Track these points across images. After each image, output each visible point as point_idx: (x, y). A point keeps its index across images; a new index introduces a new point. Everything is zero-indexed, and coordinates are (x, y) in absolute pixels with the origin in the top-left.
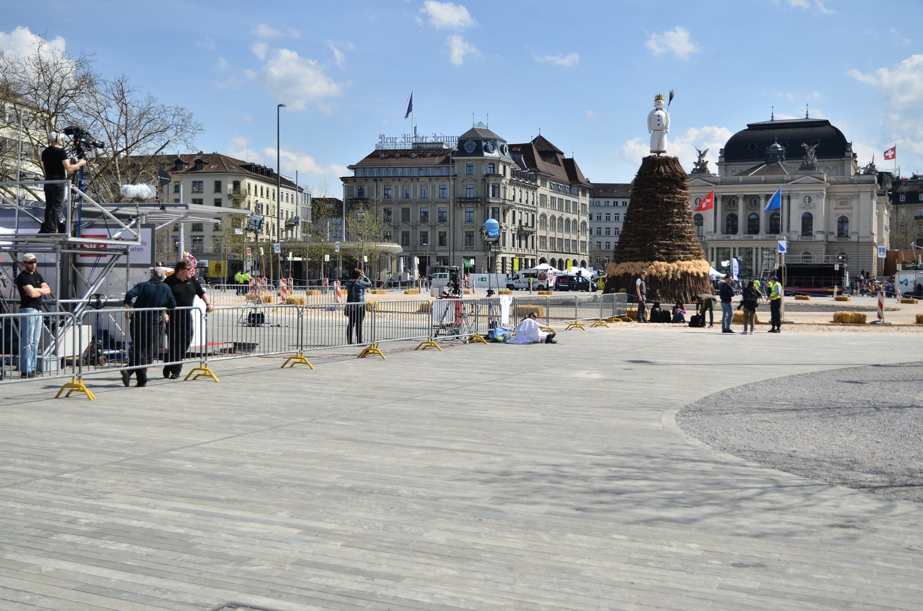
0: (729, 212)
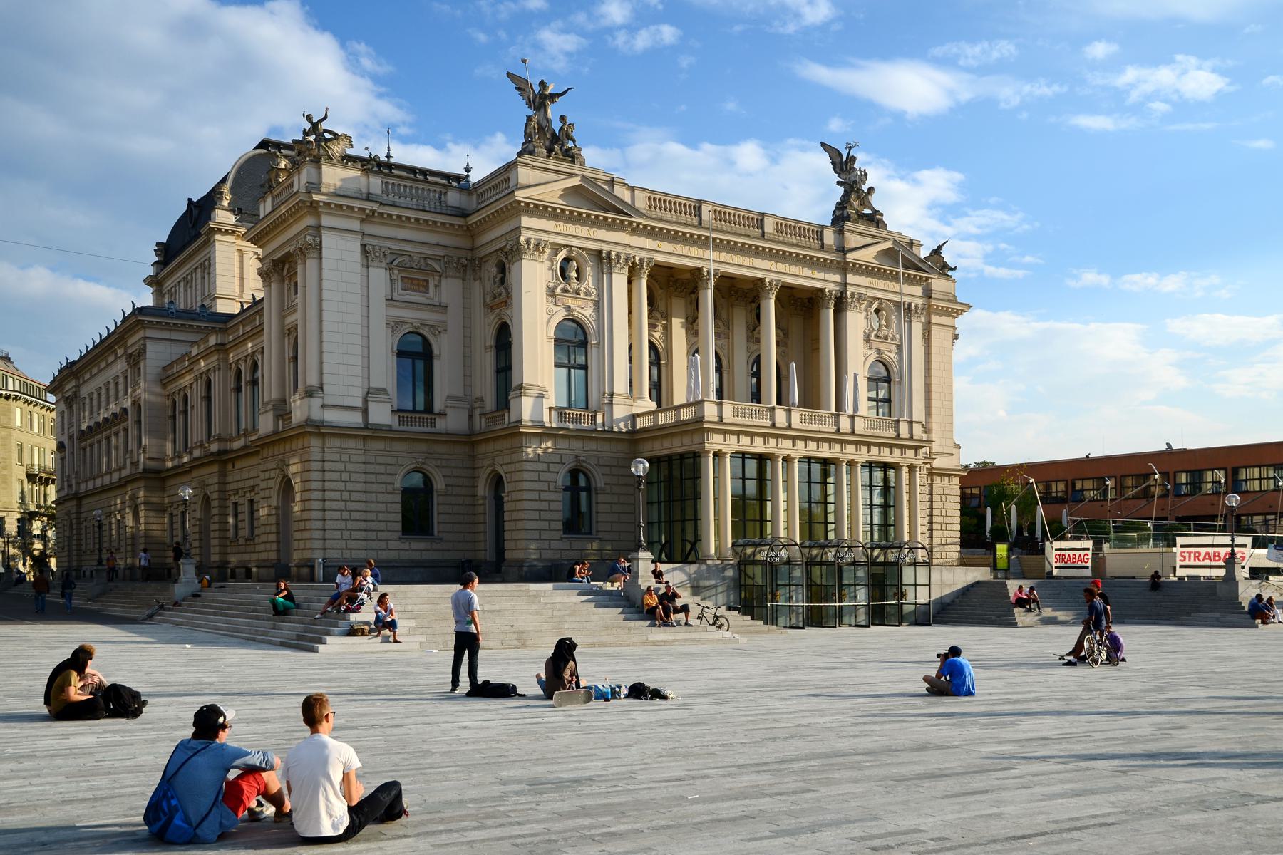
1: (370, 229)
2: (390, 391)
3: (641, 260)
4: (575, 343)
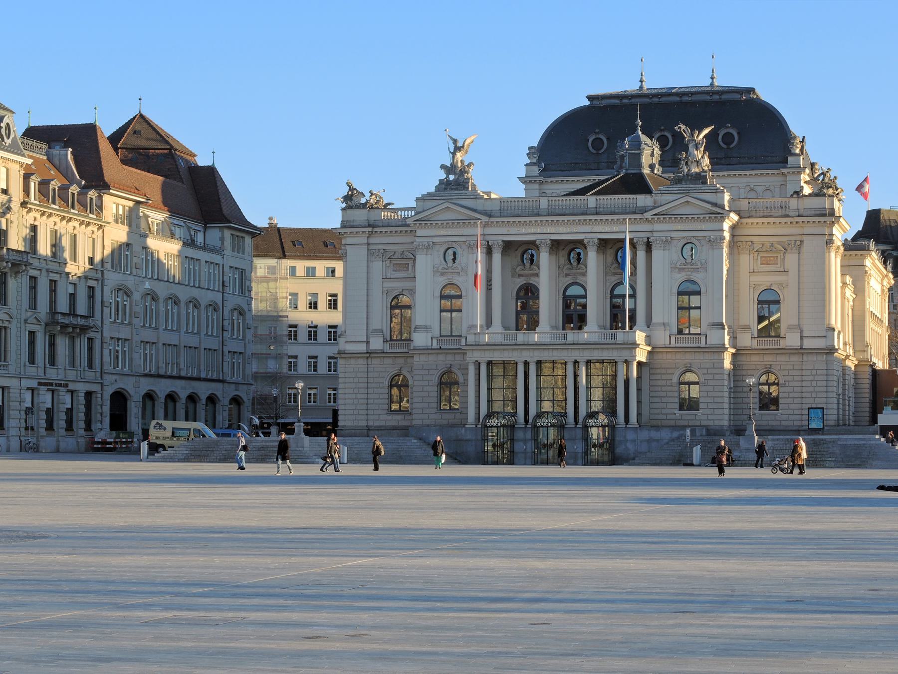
0: (521, 281)
2: (384, 331)
4: (450, 298)
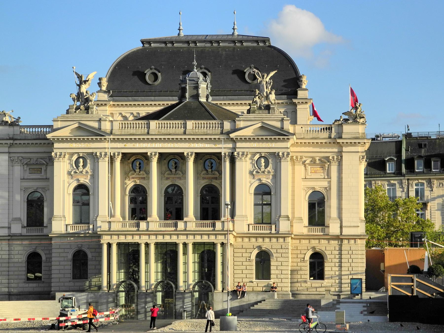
1: (12, 150)
2: (22, 219)
3: (114, 154)
